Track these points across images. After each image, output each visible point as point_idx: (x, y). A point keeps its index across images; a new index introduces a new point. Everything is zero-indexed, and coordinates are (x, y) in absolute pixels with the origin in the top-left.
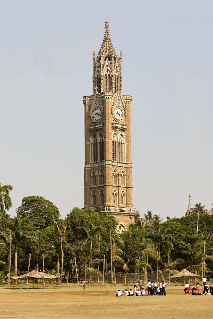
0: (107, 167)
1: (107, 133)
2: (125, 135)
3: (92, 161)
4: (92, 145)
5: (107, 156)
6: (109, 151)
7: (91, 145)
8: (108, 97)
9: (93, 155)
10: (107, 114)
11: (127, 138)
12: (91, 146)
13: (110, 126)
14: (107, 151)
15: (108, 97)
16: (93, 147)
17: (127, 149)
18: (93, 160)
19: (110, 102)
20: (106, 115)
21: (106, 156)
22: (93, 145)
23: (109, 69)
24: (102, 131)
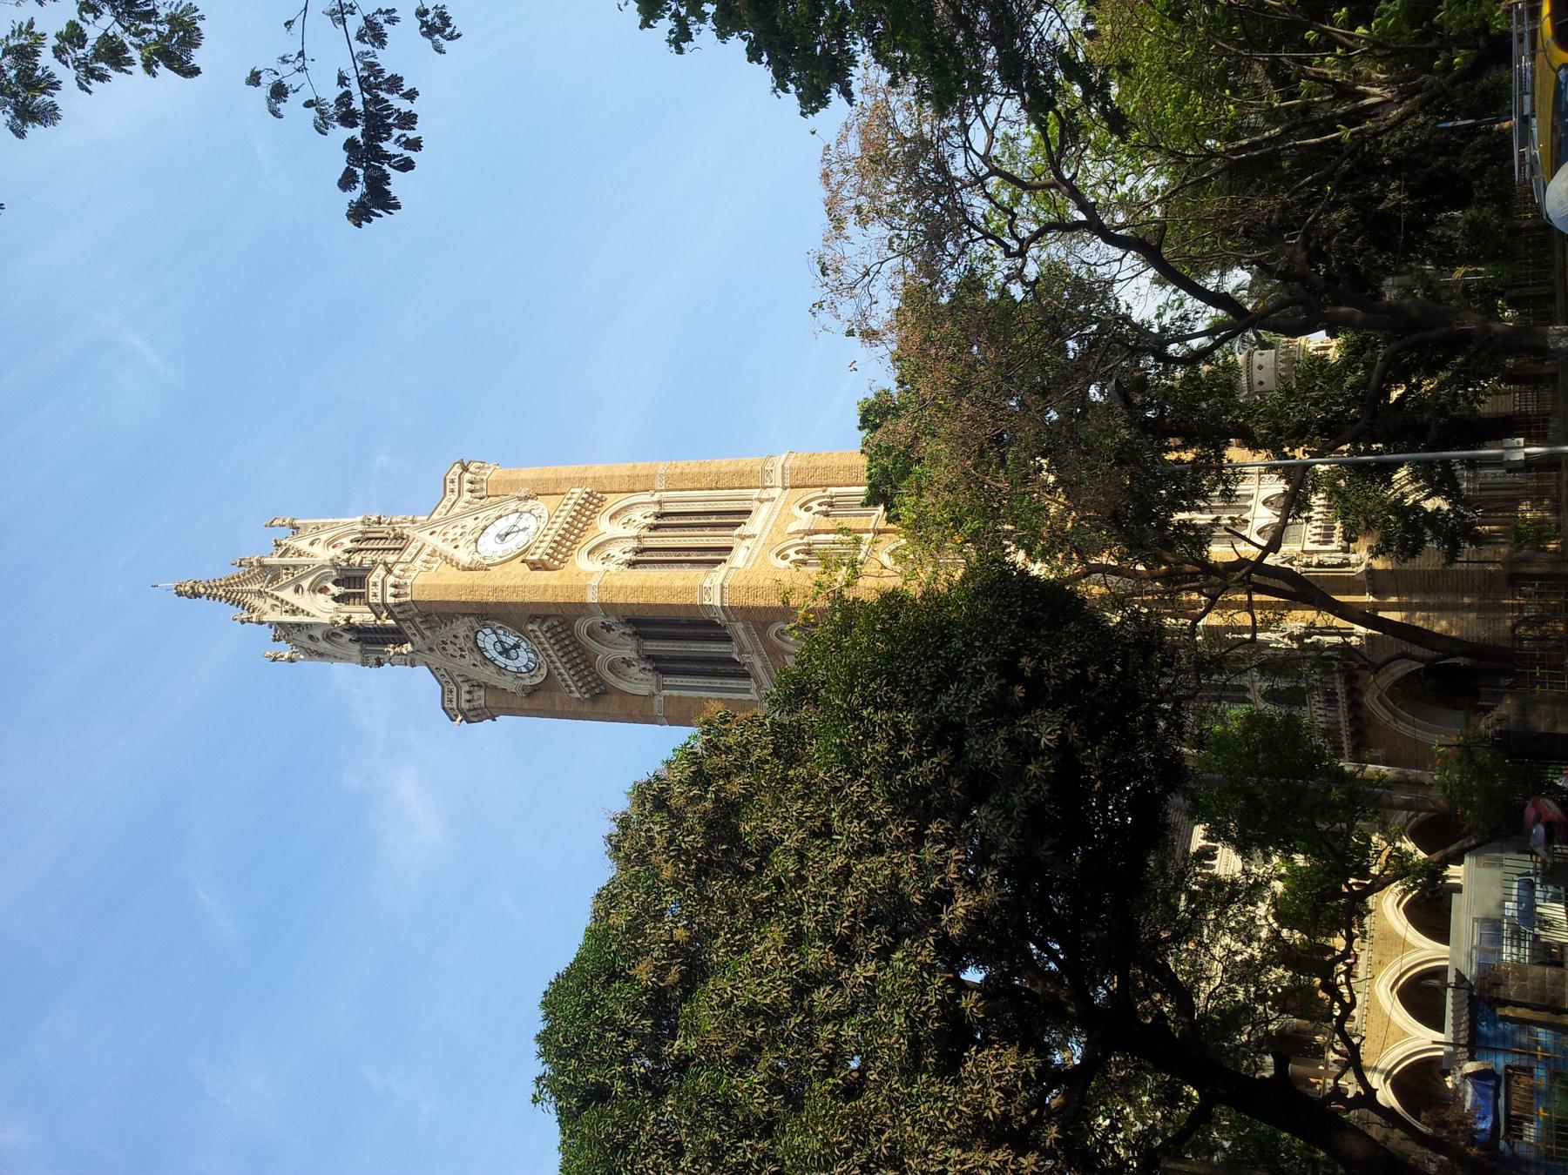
0: (736, 603)
1: (560, 600)
2: (623, 496)
3: (747, 691)
4: (665, 687)
5: (675, 601)
6: (651, 589)
7: (666, 692)
8: (391, 590)
9: (717, 682)
10: (470, 598)
11: (637, 487)
12: (675, 693)
13: (542, 577)
14: (652, 601)
15: (391, 590)
16: (678, 681)
17: (690, 485)
18: (743, 683)
19: (420, 581)
20: (477, 598)
21: (679, 607)
22: (668, 680)
23: (310, 579)
24: (559, 623)
